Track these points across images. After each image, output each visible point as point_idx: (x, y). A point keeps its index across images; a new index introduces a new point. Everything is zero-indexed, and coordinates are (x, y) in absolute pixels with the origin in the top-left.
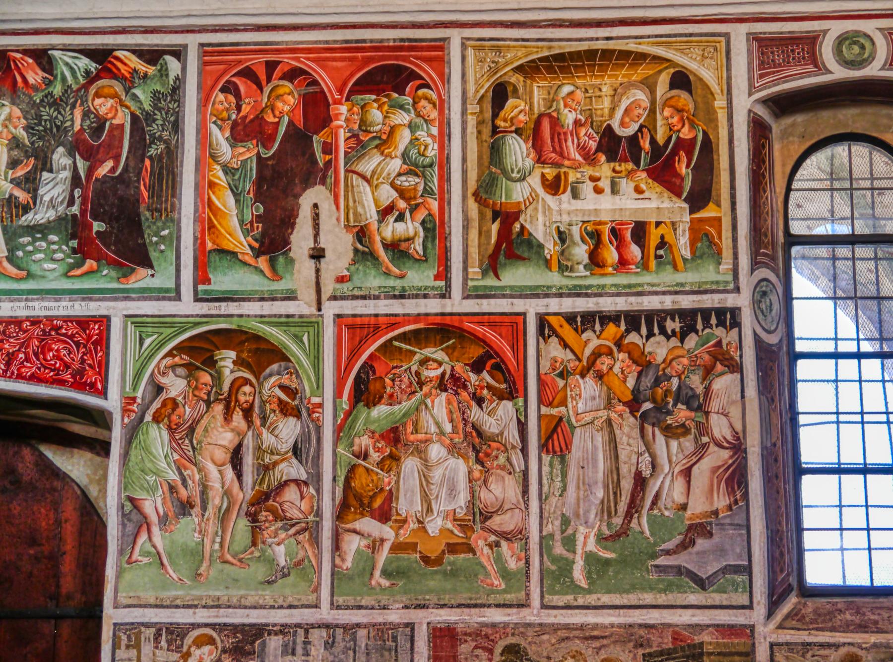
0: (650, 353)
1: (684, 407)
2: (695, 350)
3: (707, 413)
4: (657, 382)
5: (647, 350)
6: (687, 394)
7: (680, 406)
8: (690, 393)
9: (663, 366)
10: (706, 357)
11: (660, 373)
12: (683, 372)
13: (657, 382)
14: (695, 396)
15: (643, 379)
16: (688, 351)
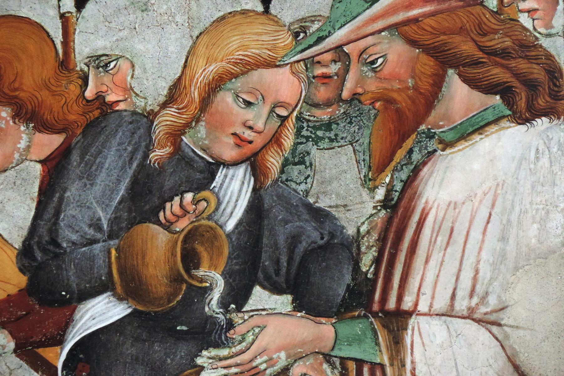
0: (101, 62)
1: (283, 302)
2: (332, 24)
3: (396, 322)
4: (144, 199)
5: (84, 47)
6: (294, 240)
7: (260, 297)
8: (312, 234)
9: (169, 118)
10: (395, 53)
11: (159, 154)
12: (275, 140)
13: (144, 199)
14: (337, 246)
15: (73, 191)
16: (298, 32)
